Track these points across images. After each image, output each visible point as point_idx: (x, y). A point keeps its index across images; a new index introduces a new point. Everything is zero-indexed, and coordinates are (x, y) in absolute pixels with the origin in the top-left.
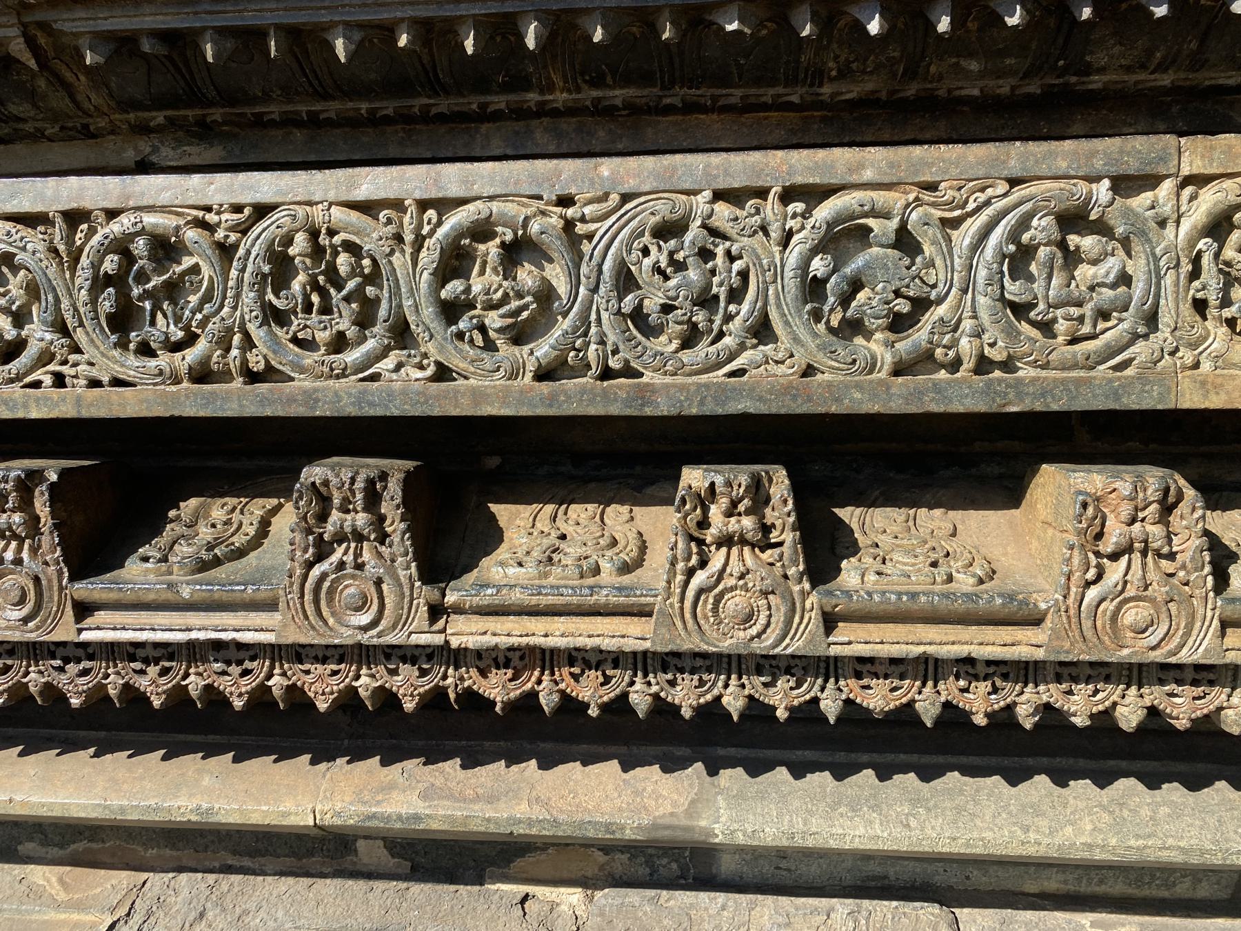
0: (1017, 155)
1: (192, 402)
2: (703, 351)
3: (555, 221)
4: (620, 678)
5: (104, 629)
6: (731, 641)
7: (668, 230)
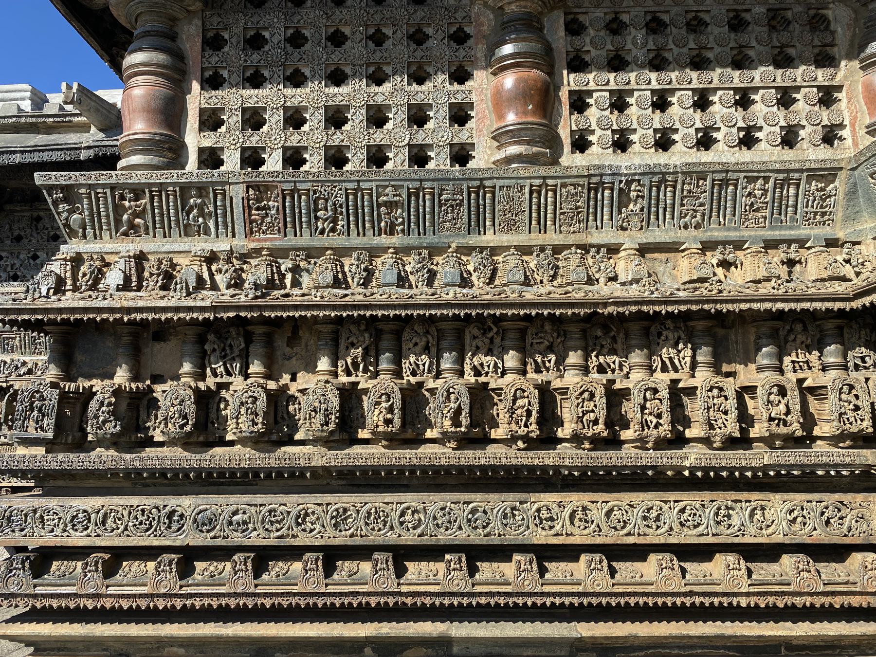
0: (504, 496)
1: (350, 542)
2: (449, 531)
3: (422, 506)
4: (434, 598)
5: (331, 589)
6: (455, 589)
7: (443, 509)
